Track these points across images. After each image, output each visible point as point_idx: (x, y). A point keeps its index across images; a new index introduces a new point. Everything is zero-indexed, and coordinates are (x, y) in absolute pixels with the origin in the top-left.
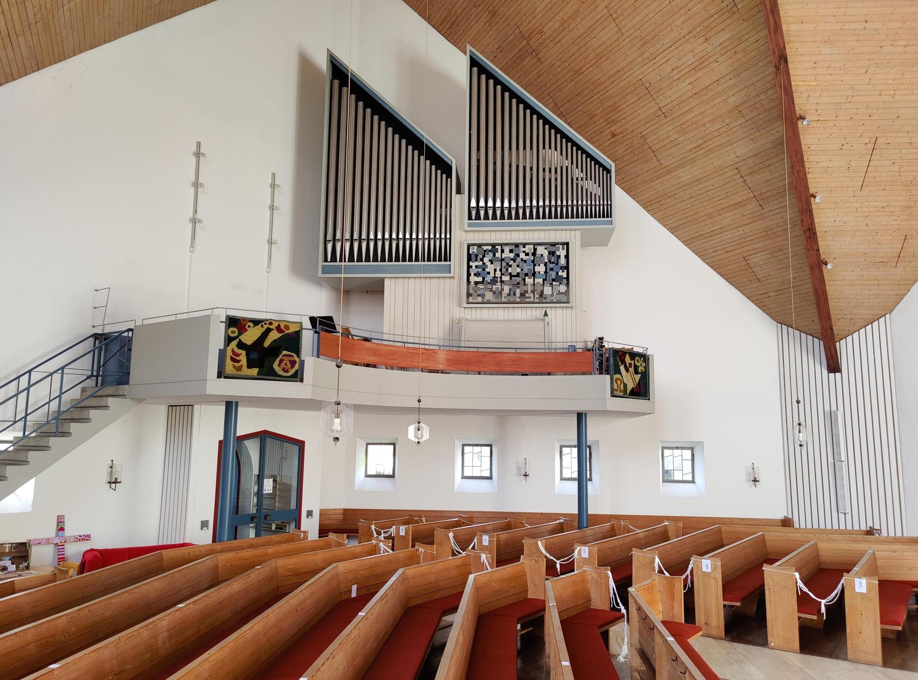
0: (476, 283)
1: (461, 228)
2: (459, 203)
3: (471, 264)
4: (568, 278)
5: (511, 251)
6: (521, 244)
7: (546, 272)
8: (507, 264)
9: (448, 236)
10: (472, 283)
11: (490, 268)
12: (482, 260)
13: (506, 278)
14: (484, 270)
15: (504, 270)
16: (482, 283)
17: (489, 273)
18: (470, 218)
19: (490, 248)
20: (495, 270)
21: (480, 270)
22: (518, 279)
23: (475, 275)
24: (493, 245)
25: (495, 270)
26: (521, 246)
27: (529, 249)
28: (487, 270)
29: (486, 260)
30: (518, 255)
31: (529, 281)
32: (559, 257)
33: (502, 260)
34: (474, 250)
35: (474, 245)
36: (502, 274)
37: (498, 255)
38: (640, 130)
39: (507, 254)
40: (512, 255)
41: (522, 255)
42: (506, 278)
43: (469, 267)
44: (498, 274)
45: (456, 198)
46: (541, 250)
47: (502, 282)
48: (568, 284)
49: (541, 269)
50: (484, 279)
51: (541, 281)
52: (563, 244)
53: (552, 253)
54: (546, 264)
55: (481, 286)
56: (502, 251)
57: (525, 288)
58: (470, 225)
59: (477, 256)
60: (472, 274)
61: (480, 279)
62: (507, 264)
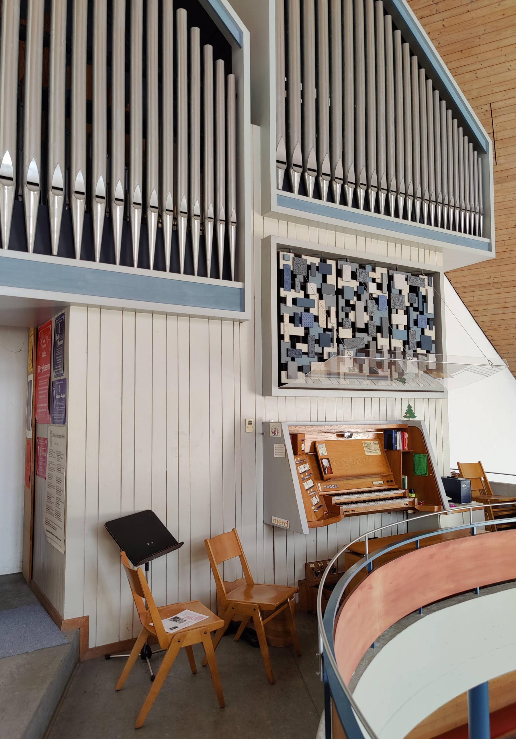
0: (295, 339)
1: (265, 209)
2: (261, 147)
3: (283, 293)
4: (438, 342)
5: (354, 276)
6: (370, 262)
7: (407, 328)
8: (347, 302)
9: (233, 217)
10: (287, 339)
11: (318, 309)
12: (304, 288)
13: (346, 333)
14: (307, 310)
15: (342, 315)
16: (305, 340)
17: (316, 319)
18: (288, 186)
19: (316, 261)
20: (328, 313)
21: (300, 310)
22: (366, 338)
23: (292, 320)
24: (324, 257)
25: (328, 313)
26: (368, 268)
27: (380, 274)
28: (313, 311)
29: (312, 288)
30: (364, 285)
31: (383, 342)
32: (425, 298)
33: (339, 292)
34: (288, 261)
35: (288, 249)
36: (340, 324)
37: (331, 279)
38: (491, 99)
39: (347, 282)
40: (354, 284)
41: (372, 288)
42: (346, 333)
43: (281, 300)
44: (333, 323)
45: (250, 132)
46: (401, 282)
47: (340, 341)
48: (439, 351)
49: (400, 319)
50: (307, 329)
51: (398, 343)
52: (429, 274)
53: (414, 290)
54: (407, 312)
55: (302, 347)
56: (339, 273)
57: (378, 358)
58: (281, 201)
59: (293, 276)
60: (287, 319)
61: (300, 331)
62: (347, 302)
